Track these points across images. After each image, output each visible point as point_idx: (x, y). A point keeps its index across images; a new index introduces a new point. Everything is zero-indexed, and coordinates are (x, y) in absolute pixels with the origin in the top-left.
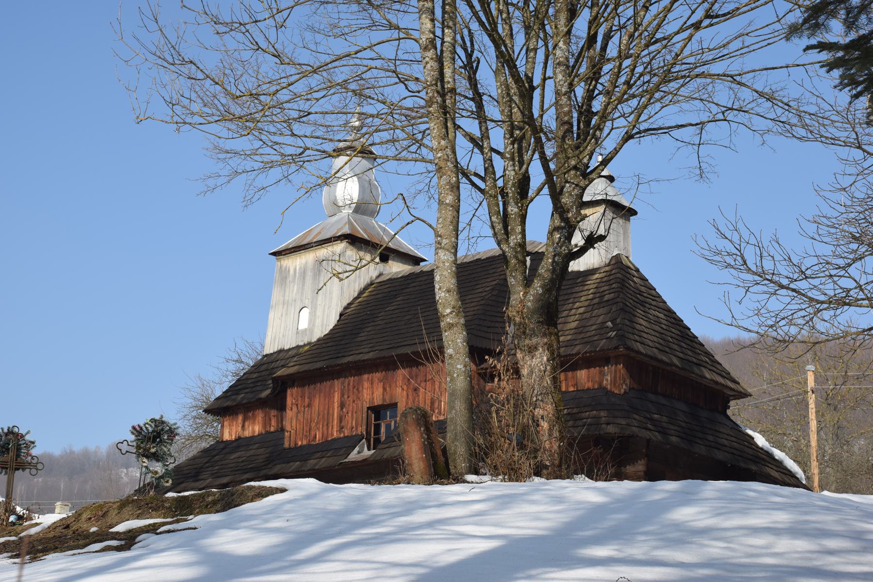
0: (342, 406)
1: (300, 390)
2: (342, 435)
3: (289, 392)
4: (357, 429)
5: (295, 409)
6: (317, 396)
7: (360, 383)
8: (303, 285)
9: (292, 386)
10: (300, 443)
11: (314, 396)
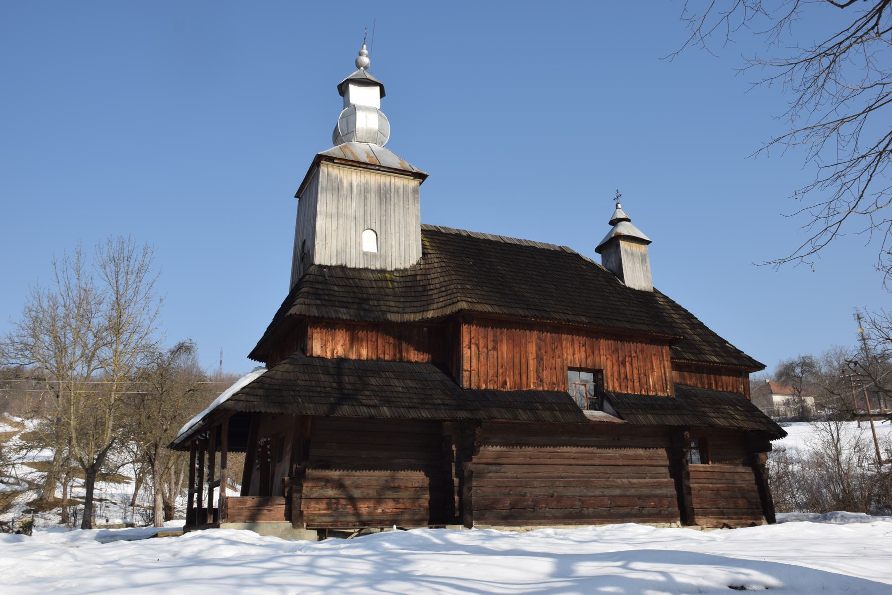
0: (539, 359)
1: (482, 330)
2: (541, 388)
3: (465, 329)
4: (558, 385)
5: (473, 347)
6: (505, 341)
7: (560, 340)
9: (469, 322)
10: (484, 387)
11: (501, 341)
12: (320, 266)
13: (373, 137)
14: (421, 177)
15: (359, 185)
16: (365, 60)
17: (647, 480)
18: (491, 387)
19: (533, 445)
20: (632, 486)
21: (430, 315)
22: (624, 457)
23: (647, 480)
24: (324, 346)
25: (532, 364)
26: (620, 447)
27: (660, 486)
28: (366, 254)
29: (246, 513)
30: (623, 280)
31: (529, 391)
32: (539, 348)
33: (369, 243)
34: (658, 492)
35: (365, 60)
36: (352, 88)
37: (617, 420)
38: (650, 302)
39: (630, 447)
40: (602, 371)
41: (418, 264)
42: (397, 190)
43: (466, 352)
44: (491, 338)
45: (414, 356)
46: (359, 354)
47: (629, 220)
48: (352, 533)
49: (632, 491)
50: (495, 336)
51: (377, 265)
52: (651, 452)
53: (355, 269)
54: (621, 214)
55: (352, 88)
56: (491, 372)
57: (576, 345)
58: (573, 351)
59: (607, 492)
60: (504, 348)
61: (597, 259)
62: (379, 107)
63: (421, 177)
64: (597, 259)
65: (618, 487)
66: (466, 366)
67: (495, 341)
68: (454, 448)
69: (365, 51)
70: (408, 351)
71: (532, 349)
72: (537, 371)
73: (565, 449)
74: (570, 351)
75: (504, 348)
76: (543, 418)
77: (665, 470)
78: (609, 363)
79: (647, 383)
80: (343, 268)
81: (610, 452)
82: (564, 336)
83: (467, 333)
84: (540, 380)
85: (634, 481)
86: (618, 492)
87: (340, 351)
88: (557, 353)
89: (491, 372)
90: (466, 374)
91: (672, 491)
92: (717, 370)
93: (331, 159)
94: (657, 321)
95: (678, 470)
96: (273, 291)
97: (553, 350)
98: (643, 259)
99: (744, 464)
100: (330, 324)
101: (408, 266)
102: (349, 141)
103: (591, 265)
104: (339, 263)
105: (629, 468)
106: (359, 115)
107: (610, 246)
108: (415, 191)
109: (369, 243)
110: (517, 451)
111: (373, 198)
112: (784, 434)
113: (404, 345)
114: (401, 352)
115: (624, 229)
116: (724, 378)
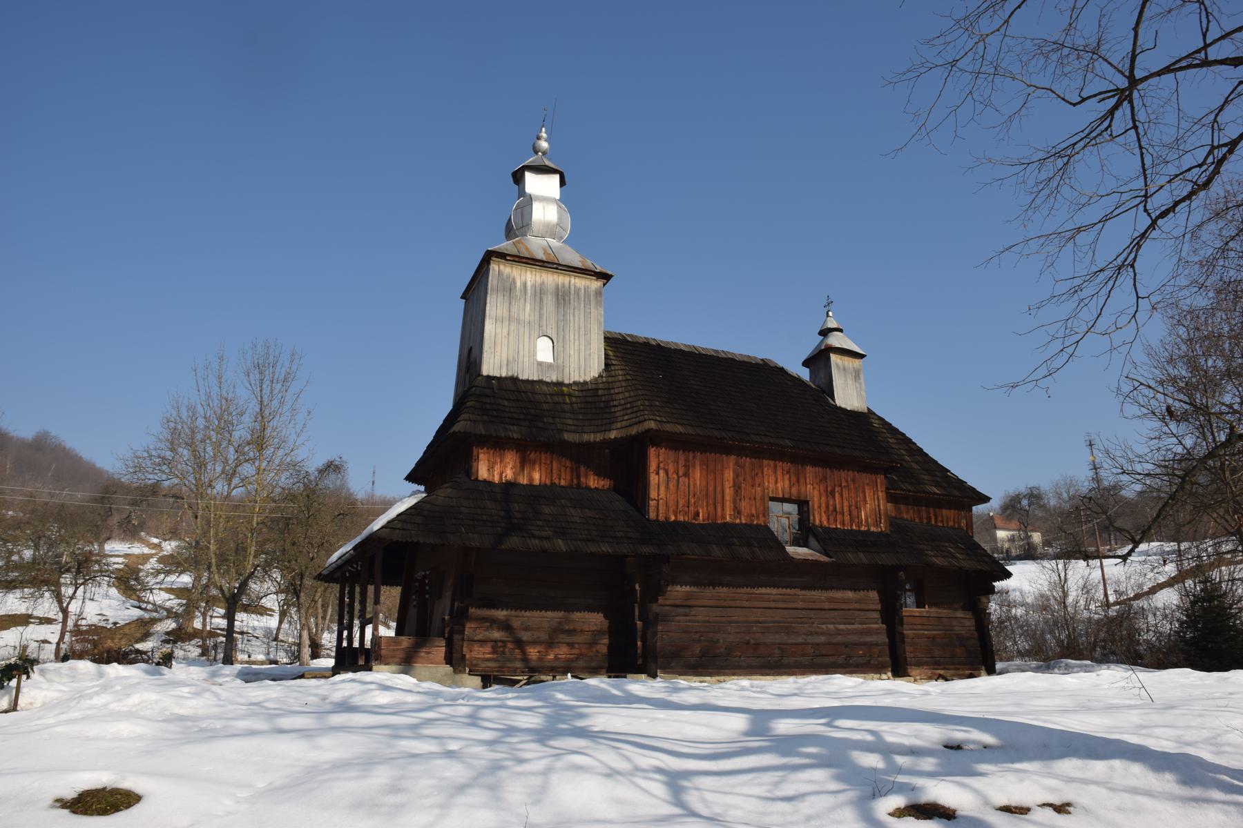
0: (737, 487)
1: (672, 453)
2: (738, 521)
3: (652, 451)
4: (758, 518)
5: (662, 473)
6: (698, 468)
8: (541, 309)
9: (658, 445)
10: (673, 518)
11: (694, 466)
12: (488, 377)
13: (551, 231)
14: (605, 277)
15: (534, 286)
16: (544, 145)
17: (856, 626)
18: (681, 518)
19: (728, 585)
20: (839, 632)
21: (613, 435)
22: (831, 600)
23: (856, 626)
24: (490, 469)
25: (729, 493)
26: (826, 589)
27: (870, 632)
28: (540, 364)
29: (401, 655)
30: (833, 399)
31: (725, 524)
32: (737, 475)
33: (544, 351)
34: (868, 639)
35: (544, 145)
36: (528, 176)
37: (824, 559)
38: (863, 421)
39: (838, 589)
40: (807, 502)
41: (600, 376)
42: (577, 291)
43: (653, 479)
44: (681, 463)
45: (593, 482)
46: (531, 479)
47: (840, 330)
48: (519, 681)
49: (839, 639)
50: (687, 460)
51: (552, 377)
52: (862, 594)
53: (527, 381)
54: (832, 324)
55: (528, 176)
56: (681, 502)
57: (779, 473)
58: (776, 479)
59: (810, 639)
60: (697, 474)
61: (805, 374)
62: (558, 197)
63: (605, 277)
64: (805, 374)
65: (823, 634)
66: (653, 494)
67: (687, 467)
68: (637, 587)
69: (544, 135)
70: (586, 476)
71: (729, 475)
72: (734, 502)
73: (763, 590)
74: (772, 479)
75: (697, 474)
76: (741, 555)
77: (876, 615)
78: (816, 493)
79: (859, 516)
80: (514, 380)
81: (815, 594)
82: (765, 462)
83: (655, 457)
84: (737, 511)
85: (842, 627)
86: (823, 639)
87: (509, 474)
88: (758, 480)
89: (681, 502)
90: (652, 503)
91: (884, 639)
92: (936, 503)
93: (502, 256)
94: (871, 446)
95: (891, 615)
96: (436, 403)
97: (753, 478)
98: (857, 374)
99: (964, 609)
100: (498, 444)
101: (588, 379)
102: (524, 235)
103: (798, 381)
104: (510, 374)
105: (836, 613)
106: (537, 207)
107: (819, 360)
108: (598, 293)
109: (544, 351)
110: (709, 592)
111: (549, 301)
112: (1008, 575)
113: (582, 469)
114: (578, 477)
115: (836, 340)
116: (944, 511)
